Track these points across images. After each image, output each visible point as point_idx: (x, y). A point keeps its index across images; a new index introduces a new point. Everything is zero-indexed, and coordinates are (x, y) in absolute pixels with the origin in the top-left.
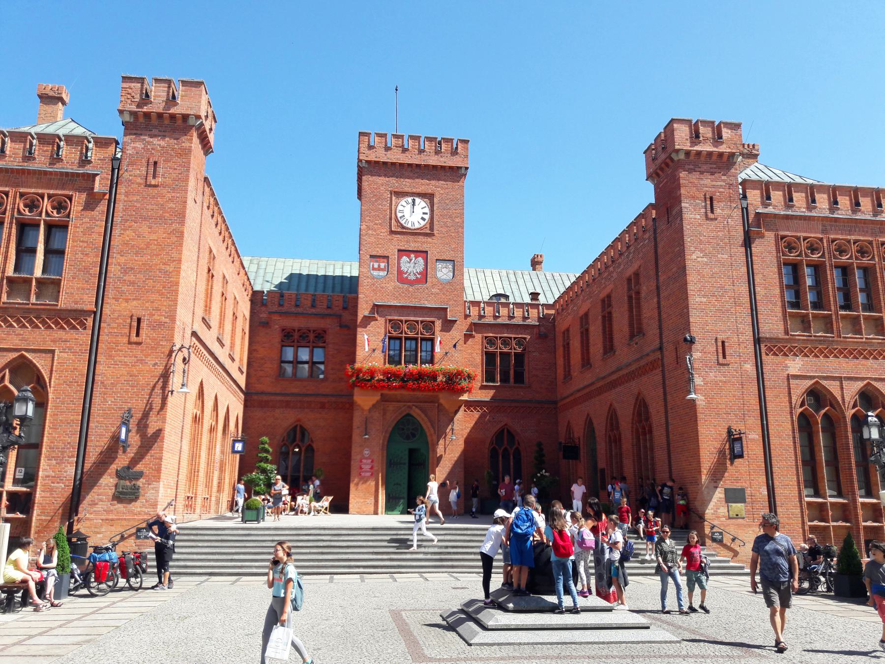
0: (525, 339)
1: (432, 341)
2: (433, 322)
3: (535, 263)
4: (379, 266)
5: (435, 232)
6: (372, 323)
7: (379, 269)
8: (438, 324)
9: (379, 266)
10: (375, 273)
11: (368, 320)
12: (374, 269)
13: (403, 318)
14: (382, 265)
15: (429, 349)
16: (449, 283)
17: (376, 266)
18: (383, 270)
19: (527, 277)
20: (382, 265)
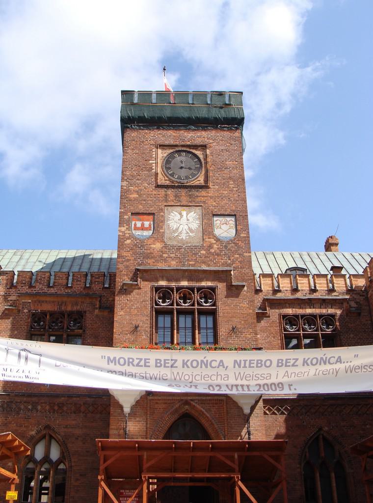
0: (333, 316)
1: (213, 313)
2: (213, 289)
3: (329, 246)
4: (143, 225)
5: (210, 184)
6: (136, 291)
7: (143, 228)
8: (221, 287)
9: (143, 225)
10: (138, 233)
11: (126, 290)
12: (136, 228)
13: (173, 284)
14: (147, 224)
15: (210, 325)
16: (232, 241)
17: (139, 224)
18: (147, 229)
19: (323, 258)
20: (147, 224)
